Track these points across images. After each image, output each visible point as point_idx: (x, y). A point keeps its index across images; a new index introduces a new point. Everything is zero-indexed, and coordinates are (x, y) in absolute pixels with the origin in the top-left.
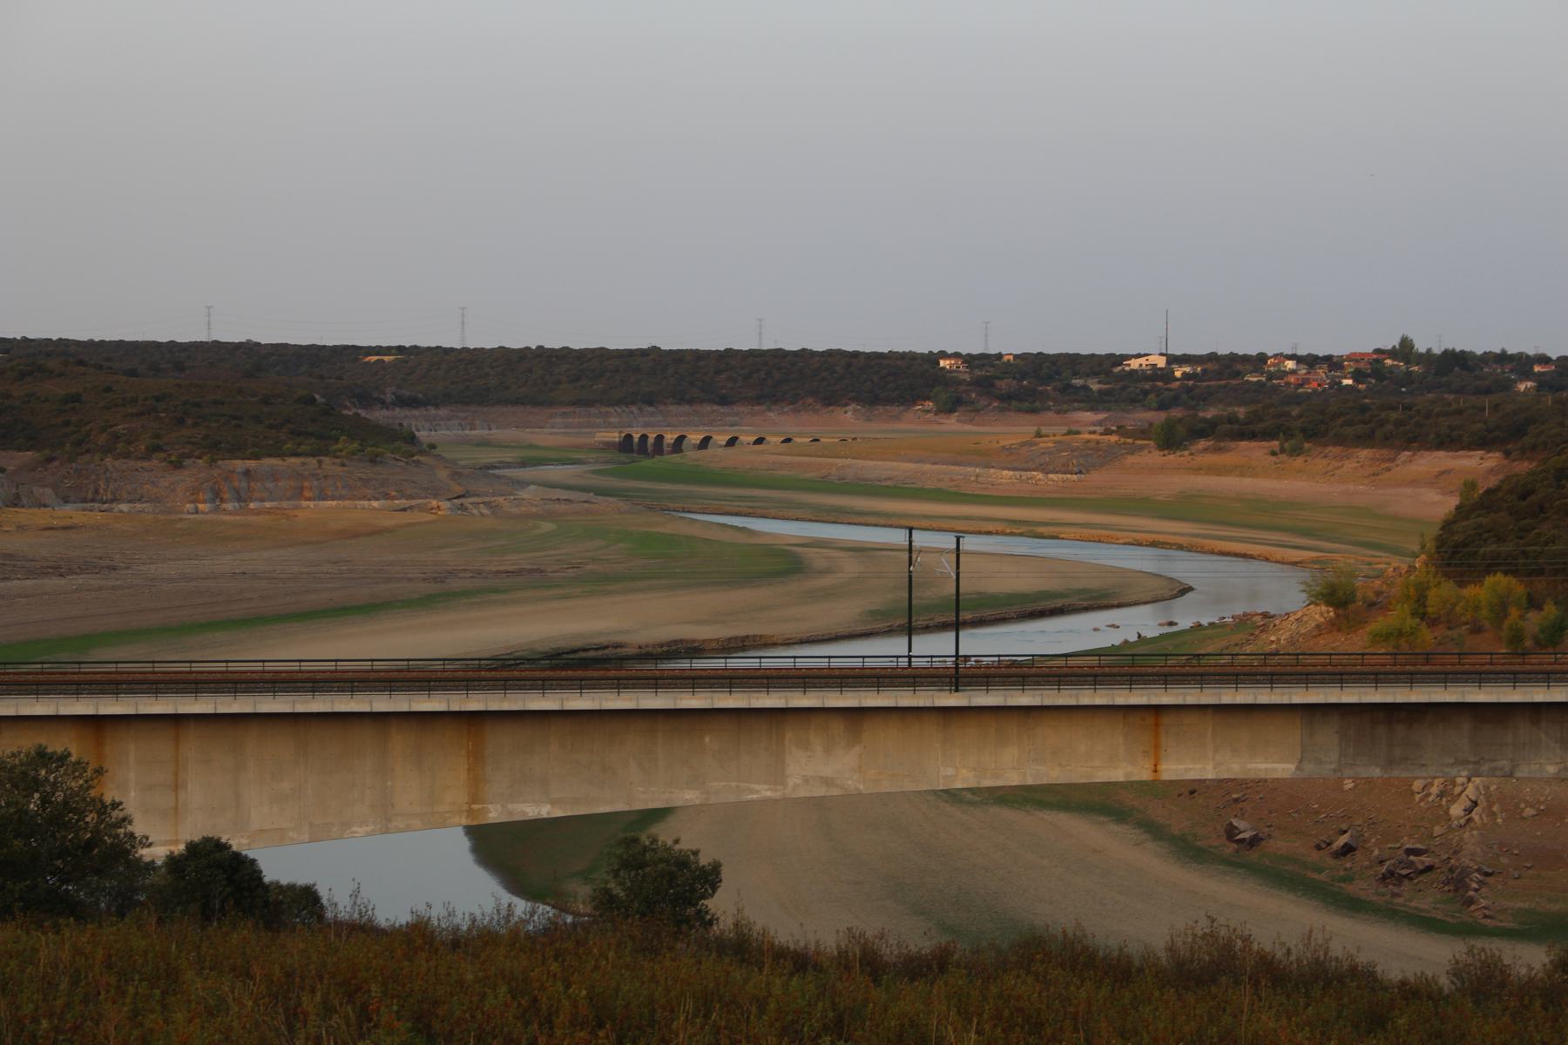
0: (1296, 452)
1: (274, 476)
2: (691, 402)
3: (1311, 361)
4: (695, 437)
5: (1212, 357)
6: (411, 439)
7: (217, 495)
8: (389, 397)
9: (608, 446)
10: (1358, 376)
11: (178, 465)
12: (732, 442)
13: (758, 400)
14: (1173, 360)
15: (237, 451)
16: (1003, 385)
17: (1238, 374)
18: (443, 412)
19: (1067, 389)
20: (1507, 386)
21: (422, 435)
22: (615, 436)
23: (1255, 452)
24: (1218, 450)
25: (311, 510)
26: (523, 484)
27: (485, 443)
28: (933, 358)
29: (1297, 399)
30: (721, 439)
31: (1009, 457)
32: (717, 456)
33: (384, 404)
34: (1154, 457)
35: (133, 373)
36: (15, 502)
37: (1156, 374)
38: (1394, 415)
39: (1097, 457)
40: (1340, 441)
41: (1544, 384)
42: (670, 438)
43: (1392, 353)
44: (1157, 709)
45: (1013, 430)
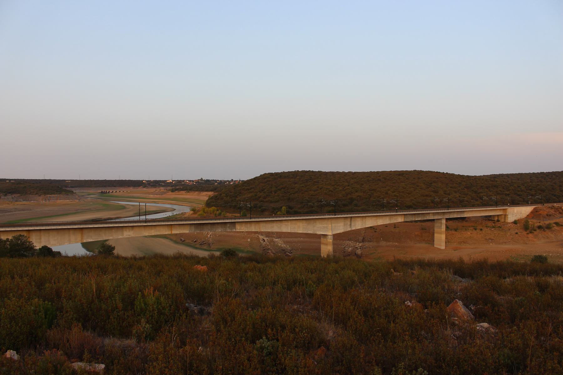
0: (188, 192)
1: (54, 197)
2: (111, 187)
3: (190, 181)
4: (111, 191)
5: (178, 180)
6: (73, 192)
7: (46, 200)
8: (69, 187)
9: (100, 192)
10: (196, 183)
11: (40, 196)
12: (116, 192)
13: (120, 186)
14: (173, 181)
15: (48, 194)
16: (151, 184)
17: (181, 183)
18: (77, 188)
19: (159, 184)
20: (214, 184)
21: (74, 191)
22: (100, 191)
23: (183, 192)
24: (179, 192)
25: (59, 201)
26: (88, 198)
27: (83, 192)
28: (142, 181)
29: (189, 186)
30: (115, 191)
31: (152, 193)
32: (114, 194)
33: (69, 188)
34: (171, 193)
35: (33, 183)
36: (17, 201)
37: (172, 183)
38: (200, 187)
39: (165, 193)
40: (194, 191)
41: (218, 183)
42: (108, 191)
43: (200, 180)
44: (171, 225)
45: (153, 190)
